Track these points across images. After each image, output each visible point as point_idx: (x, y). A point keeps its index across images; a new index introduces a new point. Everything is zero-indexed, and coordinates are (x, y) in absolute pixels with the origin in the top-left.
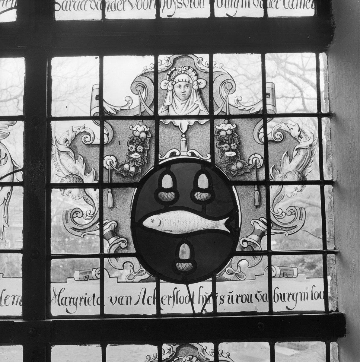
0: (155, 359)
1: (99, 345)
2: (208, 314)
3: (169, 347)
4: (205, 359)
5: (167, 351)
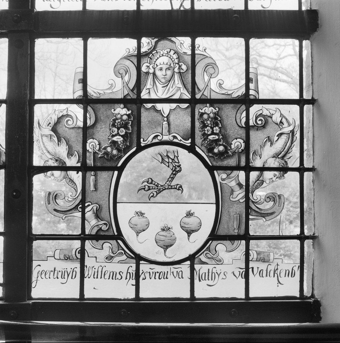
0: (135, 52)
1: (81, 39)
2: (186, 11)
4: (182, 53)
5: (145, 44)
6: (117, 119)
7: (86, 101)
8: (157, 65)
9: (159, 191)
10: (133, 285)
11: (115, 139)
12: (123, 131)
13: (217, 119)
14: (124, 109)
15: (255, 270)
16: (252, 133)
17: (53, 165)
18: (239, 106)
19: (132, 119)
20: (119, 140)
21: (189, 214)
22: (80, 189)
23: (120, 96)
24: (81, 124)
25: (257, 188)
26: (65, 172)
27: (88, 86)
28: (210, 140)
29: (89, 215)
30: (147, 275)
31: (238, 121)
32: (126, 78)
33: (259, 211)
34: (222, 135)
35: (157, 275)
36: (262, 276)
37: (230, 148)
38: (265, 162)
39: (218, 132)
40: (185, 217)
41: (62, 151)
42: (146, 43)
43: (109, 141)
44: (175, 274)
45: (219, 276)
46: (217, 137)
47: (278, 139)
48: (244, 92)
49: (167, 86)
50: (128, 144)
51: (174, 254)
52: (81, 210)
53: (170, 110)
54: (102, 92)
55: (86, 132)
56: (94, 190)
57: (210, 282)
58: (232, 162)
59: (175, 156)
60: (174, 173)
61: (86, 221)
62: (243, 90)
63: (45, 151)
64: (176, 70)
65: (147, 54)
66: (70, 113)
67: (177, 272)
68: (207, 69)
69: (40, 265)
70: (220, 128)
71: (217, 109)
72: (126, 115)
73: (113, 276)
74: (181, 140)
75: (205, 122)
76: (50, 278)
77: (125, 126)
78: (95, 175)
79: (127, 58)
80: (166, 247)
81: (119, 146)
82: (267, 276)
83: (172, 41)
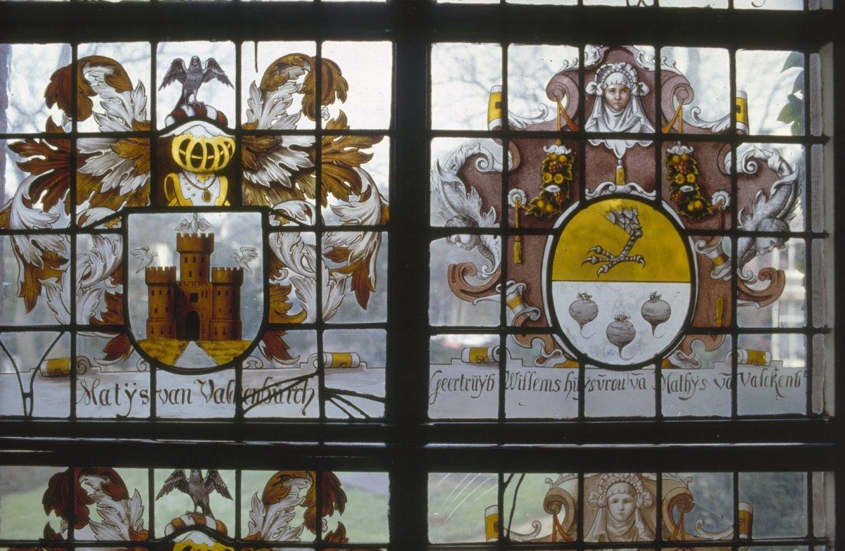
0: (575, 65)
3: (594, 49)
5: (591, 55)
6: (551, 161)
7: (506, 134)
8: (607, 84)
9: (612, 265)
10: (575, 399)
11: (549, 189)
12: (560, 178)
13: (692, 163)
14: (560, 147)
15: (746, 377)
16: (741, 184)
17: (459, 225)
18: (722, 145)
19: (573, 161)
20: (554, 191)
21: (654, 298)
22: (498, 263)
23: (555, 128)
24: (499, 167)
25: (748, 260)
26: (477, 236)
27: (509, 114)
28: (682, 192)
29: (511, 297)
30: (595, 385)
31: (721, 165)
32: (564, 102)
33: (752, 294)
34: (699, 186)
35: (610, 384)
36: (756, 386)
37: (709, 204)
38: (759, 225)
39: (693, 180)
40: (649, 301)
41: (473, 205)
42: (592, 53)
43: (541, 192)
44: (635, 382)
45: (695, 385)
46: (692, 189)
47: (776, 192)
48: (729, 126)
49: (622, 114)
50: (568, 197)
51: (630, 355)
52: (500, 291)
53: (627, 149)
54: (529, 122)
55: (508, 179)
56: (520, 262)
57: (684, 395)
58: (713, 224)
59: (633, 215)
60: (633, 238)
61: (507, 307)
62: (727, 123)
63: (448, 206)
64: (634, 91)
65: (593, 69)
66: (483, 151)
67: (637, 380)
68: (677, 91)
69: (440, 372)
70: (696, 176)
71: (692, 148)
72: (564, 154)
73: (547, 386)
74: (642, 193)
75: (676, 167)
76: (455, 389)
77: (563, 171)
78: (522, 241)
79: (565, 73)
80: (621, 344)
81: (554, 198)
82: (761, 385)
83: (628, 52)
